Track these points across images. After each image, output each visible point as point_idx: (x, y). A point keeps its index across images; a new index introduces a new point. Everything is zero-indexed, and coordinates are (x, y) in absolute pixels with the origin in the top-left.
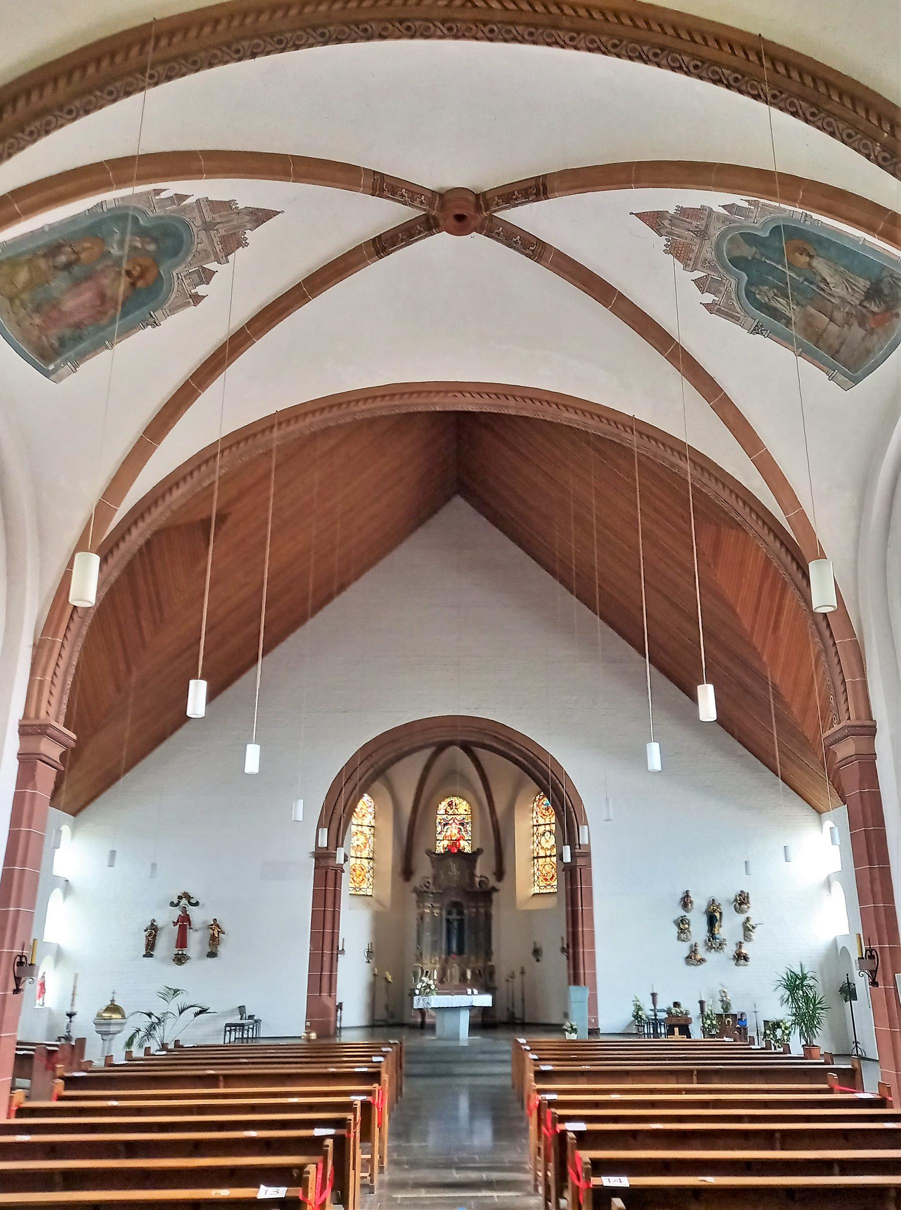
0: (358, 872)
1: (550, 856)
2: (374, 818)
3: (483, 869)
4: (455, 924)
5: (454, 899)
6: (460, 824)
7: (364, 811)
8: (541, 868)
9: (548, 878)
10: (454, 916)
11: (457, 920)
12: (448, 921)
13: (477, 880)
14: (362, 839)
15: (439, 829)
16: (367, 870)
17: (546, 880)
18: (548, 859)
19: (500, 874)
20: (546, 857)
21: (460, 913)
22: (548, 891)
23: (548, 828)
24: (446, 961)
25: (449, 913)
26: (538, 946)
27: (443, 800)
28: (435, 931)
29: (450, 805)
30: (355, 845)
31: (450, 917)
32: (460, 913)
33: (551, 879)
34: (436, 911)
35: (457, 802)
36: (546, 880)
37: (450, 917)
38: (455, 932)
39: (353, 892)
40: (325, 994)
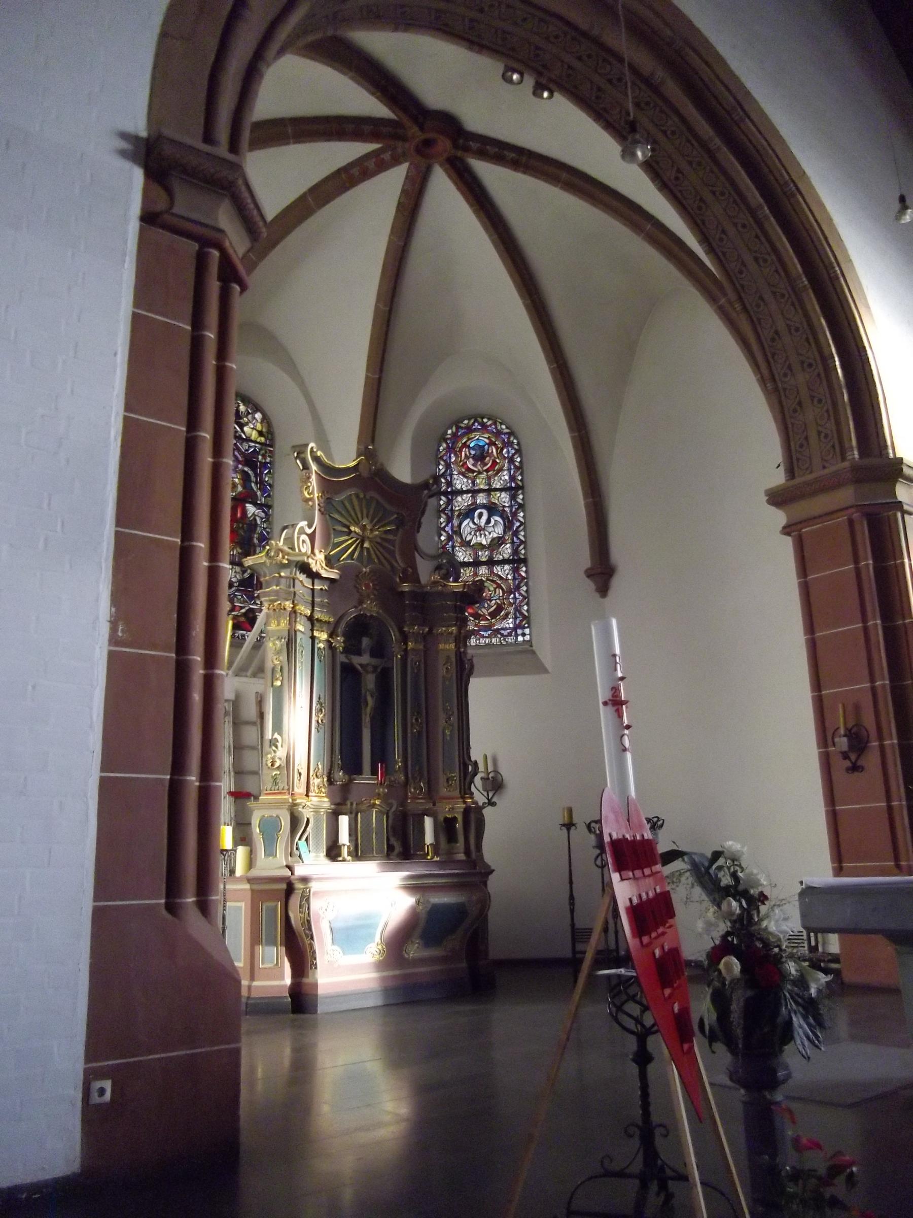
1: (491, 563)
5: (371, 607)
10: (365, 659)
20: (476, 564)
21: (379, 651)
23: (481, 499)
31: (357, 660)
32: (379, 651)
33: (494, 615)
37: (357, 660)
40: (193, 916)
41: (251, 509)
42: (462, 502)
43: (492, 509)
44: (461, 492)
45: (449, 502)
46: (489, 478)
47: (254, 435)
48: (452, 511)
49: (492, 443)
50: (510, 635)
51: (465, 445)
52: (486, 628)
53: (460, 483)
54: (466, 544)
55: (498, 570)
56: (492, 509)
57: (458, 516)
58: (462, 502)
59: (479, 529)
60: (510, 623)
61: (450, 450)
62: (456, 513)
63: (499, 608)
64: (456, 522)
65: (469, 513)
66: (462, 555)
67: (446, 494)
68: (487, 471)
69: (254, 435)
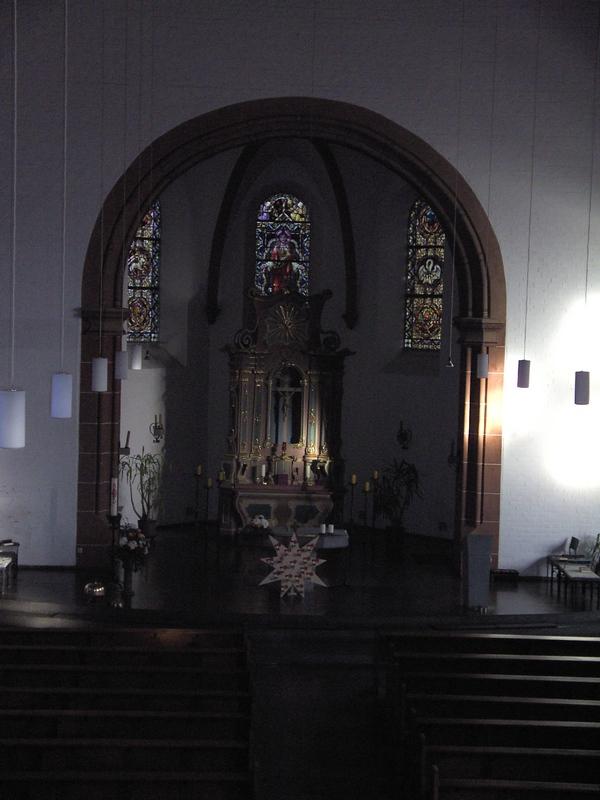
0: (138, 310)
1: (433, 296)
3: (331, 318)
6: (293, 237)
10: (286, 388)
11: (290, 392)
12: (277, 396)
13: (322, 337)
15: (260, 243)
18: (428, 301)
19: (351, 318)
20: (425, 296)
25: (278, 383)
29: (278, 206)
30: (132, 268)
31: (279, 389)
34: (259, 382)
35: (289, 202)
36: (424, 331)
37: (279, 389)
41: (295, 265)
42: (421, 253)
44: (420, 247)
45: (414, 253)
46: (436, 238)
47: (297, 218)
48: (415, 259)
52: (427, 339)
53: (421, 241)
58: (421, 253)
59: (428, 273)
61: (417, 216)
65: (423, 262)
66: (419, 290)
67: (412, 247)
69: (297, 218)
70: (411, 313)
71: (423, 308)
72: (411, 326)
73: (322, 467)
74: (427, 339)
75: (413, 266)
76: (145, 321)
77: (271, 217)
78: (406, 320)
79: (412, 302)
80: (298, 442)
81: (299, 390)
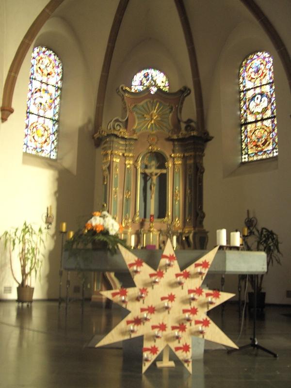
1: (262, 120)
2: (62, 80)
4: (155, 178)
7: (50, 70)
8: (249, 134)
9: (260, 143)
10: (153, 170)
11: (156, 174)
12: (145, 177)
14: (46, 97)
16: (51, 131)
17: (257, 146)
18: (259, 124)
20: (256, 121)
22: (259, 158)
23: (258, 91)
24: (142, 224)
26: (251, 216)
27: (140, 71)
28: (126, 188)
29: (146, 76)
33: (264, 144)
34: (129, 163)
36: (257, 146)
37: (148, 171)
38: (154, 188)
39: (34, 152)
42: (250, 94)
43: (262, 94)
44: (249, 90)
45: (245, 95)
46: (261, 80)
48: (246, 99)
49: (261, 64)
50: (270, 153)
51: (250, 67)
52: (261, 151)
54: (252, 113)
55: (265, 123)
56: (262, 94)
57: (248, 100)
58: (250, 94)
59: (257, 105)
60: (270, 148)
62: (247, 100)
63: (266, 141)
64: (247, 104)
66: (251, 118)
67: (243, 91)
68: (260, 77)
70: (246, 137)
71: (255, 130)
72: (246, 145)
73: (187, 238)
74: (261, 151)
75: (245, 103)
76: (46, 141)
77: (141, 83)
78: (242, 142)
79: (246, 128)
80: (164, 217)
81: (164, 171)
